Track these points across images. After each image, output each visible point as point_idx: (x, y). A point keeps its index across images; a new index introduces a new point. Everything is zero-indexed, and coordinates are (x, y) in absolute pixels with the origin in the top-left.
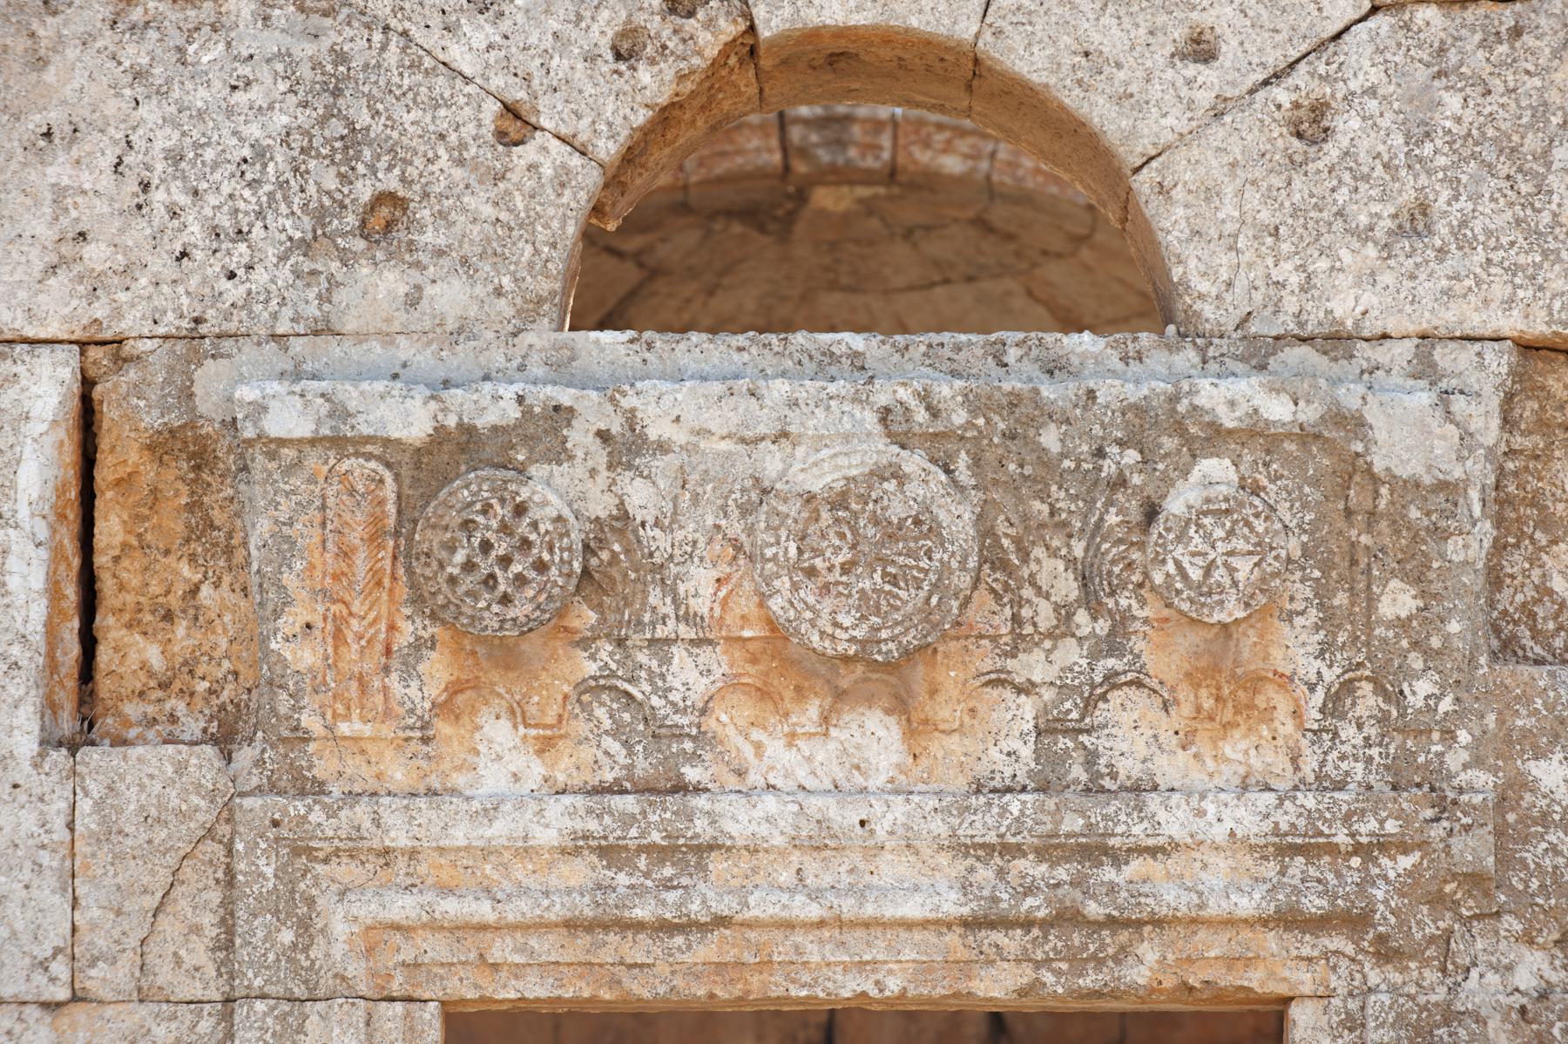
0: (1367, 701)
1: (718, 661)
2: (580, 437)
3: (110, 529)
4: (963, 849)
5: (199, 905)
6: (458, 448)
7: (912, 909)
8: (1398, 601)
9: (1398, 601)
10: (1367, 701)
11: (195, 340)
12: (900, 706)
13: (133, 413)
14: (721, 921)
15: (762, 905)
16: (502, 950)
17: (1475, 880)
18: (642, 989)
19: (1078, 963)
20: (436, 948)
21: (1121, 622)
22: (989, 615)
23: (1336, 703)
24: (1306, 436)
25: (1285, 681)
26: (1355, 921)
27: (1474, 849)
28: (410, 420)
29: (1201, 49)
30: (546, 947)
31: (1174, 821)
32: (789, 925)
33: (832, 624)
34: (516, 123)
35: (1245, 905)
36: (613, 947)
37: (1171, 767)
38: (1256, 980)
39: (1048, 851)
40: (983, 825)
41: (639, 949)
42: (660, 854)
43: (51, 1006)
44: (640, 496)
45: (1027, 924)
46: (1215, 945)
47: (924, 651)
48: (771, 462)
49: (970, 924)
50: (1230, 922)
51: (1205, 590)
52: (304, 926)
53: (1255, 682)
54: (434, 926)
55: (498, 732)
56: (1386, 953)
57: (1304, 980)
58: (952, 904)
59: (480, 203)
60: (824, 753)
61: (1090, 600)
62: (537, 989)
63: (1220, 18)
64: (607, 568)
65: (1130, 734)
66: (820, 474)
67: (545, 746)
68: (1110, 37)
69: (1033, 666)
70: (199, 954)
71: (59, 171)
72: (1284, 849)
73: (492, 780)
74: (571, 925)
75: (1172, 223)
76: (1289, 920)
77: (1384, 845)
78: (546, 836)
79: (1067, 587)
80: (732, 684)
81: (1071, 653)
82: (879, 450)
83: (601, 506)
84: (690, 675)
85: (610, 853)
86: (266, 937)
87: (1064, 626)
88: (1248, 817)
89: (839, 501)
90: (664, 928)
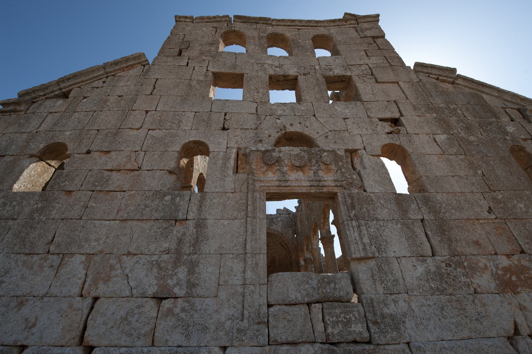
0: (339, 171)
1: (288, 168)
2: (276, 151)
3: (239, 162)
4: (309, 181)
5: (245, 185)
6: (267, 151)
7: (305, 185)
8: (341, 164)
9: (341, 164)
10: (339, 171)
11: (246, 148)
12: (302, 171)
13: (241, 152)
14: (289, 186)
15: (293, 184)
16: (271, 188)
17: (351, 183)
18: (283, 191)
19: (319, 189)
20: (265, 188)
21: (319, 165)
22: (309, 164)
23: (337, 171)
24: (332, 151)
25: (333, 169)
26: (342, 186)
27: (350, 181)
28: (263, 149)
29: (318, 133)
30: (275, 188)
31: (326, 179)
32: (295, 186)
33: (297, 164)
34: (270, 136)
35: (333, 185)
36: (280, 188)
37: (324, 176)
38: (334, 191)
39: (316, 181)
40: (310, 179)
41: (283, 188)
42: (284, 181)
43: (232, 193)
44: (281, 155)
45: (315, 186)
46: (331, 188)
47: (304, 166)
48: (291, 152)
49: (310, 186)
50: (332, 186)
51: (326, 161)
52: (254, 186)
53: (330, 169)
54: (265, 186)
55: (270, 173)
56: (345, 189)
57: (338, 191)
58: (309, 185)
59: (267, 140)
60: (297, 174)
61: (317, 163)
62: (274, 191)
63: (319, 131)
64: (278, 161)
65: (321, 173)
66: (295, 153)
67: (274, 174)
68: (312, 132)
69: (313, 168)
70: (245, 189)
71: (236, 138)
72: (335, 181)
73: (270, 176)
74: (277, 186)
75: (318, 142)
76: (336, 186)
77: (343, 181)
78: (275, 179)
79: (315, 162)
80: (289, 169)
81: (316, 167)
82: (300, 151)
83: (278, 156)
84: (285, 169)
85: (280, 181)
86: (251, 187)
87: (315, 165)
88: (332, 178)
89: (297, 155)
90: (285, 186)
